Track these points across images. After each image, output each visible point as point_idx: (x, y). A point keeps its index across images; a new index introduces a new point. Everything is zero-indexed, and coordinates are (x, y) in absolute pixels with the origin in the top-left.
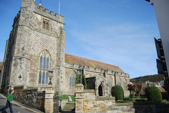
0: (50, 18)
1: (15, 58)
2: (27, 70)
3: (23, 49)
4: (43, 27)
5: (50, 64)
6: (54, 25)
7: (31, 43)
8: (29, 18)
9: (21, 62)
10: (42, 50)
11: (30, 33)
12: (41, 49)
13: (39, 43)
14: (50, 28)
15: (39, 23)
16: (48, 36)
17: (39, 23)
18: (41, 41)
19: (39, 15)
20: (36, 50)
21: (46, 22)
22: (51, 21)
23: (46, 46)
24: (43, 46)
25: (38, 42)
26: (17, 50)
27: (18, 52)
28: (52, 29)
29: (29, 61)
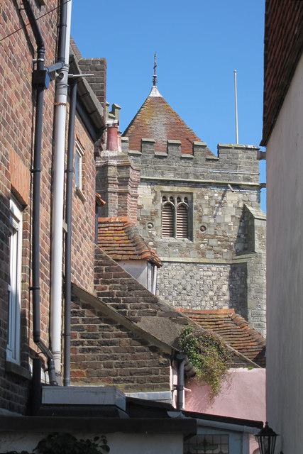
0: (191, 179)
14: (196, 226)
16: (188, 267)
21: (176, 205)
22: (196, 192)
28: (203, 228)
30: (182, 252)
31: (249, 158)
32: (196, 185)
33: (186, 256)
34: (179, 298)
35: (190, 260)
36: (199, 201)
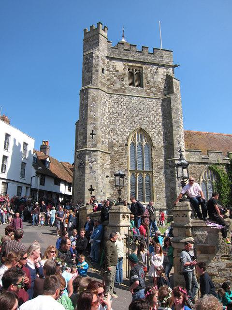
3: (93, 134)
7: (107, 121)
8: (98, 71)
10: (131, 131)
14: (145, 82)
15: (121, 77)
16: (142, 99)
21: (135, 72)
22: (144, 66)
24: (133, 123)
26: (82, 137)
28: (148, 83)
29: (107, 157)
32: (144, 63)
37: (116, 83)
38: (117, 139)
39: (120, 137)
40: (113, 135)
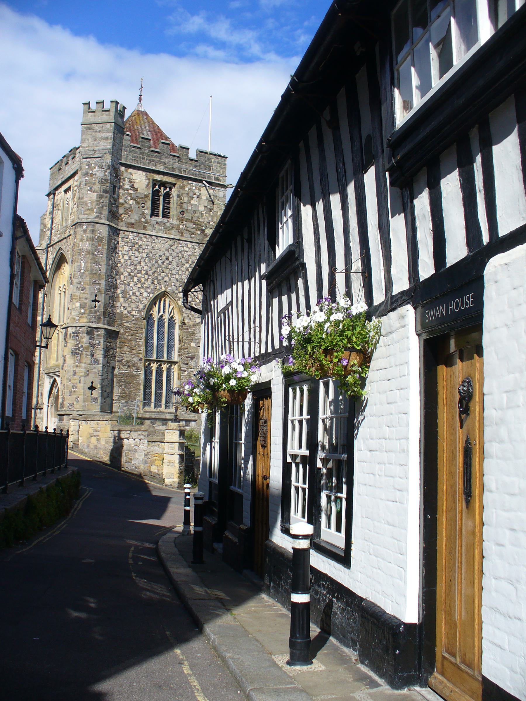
0: (176, 173)
1: (74, 329)
2: (112, 365)
4: (154, 213)
5: (180, 341)
6: (192, 198)
9: (94, 342)
11: (112, 245)
12: (149, 290)
13: (143, 272)
16: (170, 242)
17: (140, 201)
18: (150, 265)
19: (140, 172)
20: (134, 297)
22: (179, 183)
23: (166, 279)
24: (156, 282)
25: (139, 268)
26: (78, 304)
27: (82, 311)
30: (168, 230)
31: (219, 163)
33: (169, 233)
34: (163, 266)
35: (172, 237)
36: (181, 191)
37: (131, 211)
38: (129, 309)
39: (133, 306)
40: (125, 301)
